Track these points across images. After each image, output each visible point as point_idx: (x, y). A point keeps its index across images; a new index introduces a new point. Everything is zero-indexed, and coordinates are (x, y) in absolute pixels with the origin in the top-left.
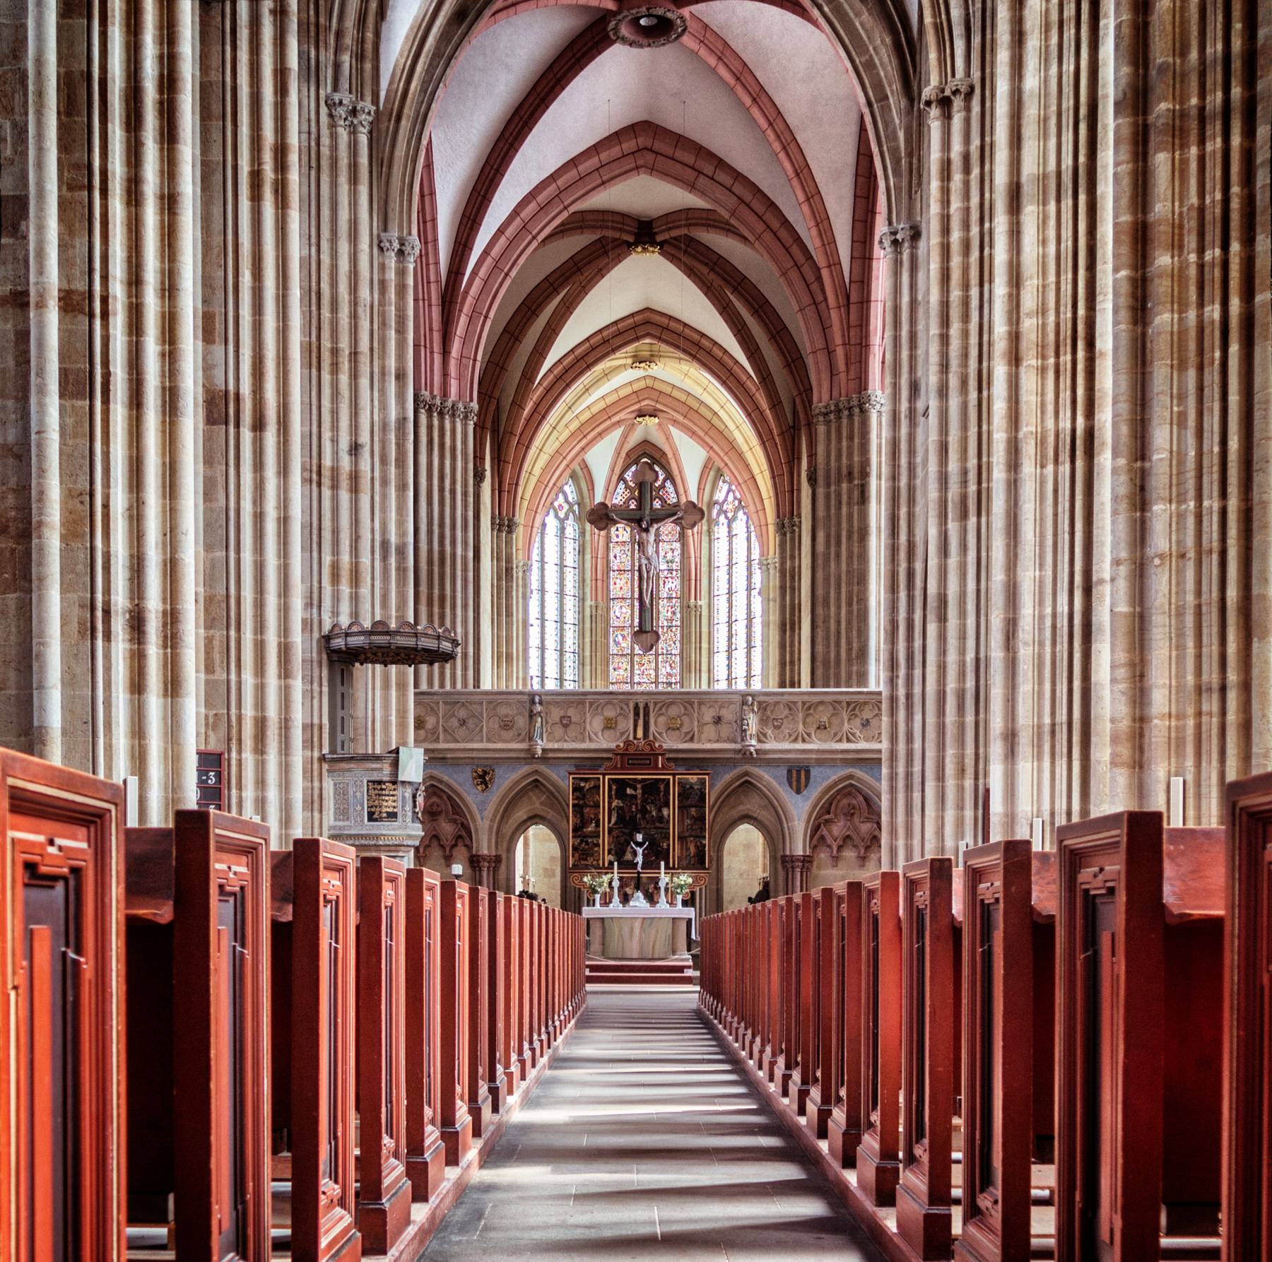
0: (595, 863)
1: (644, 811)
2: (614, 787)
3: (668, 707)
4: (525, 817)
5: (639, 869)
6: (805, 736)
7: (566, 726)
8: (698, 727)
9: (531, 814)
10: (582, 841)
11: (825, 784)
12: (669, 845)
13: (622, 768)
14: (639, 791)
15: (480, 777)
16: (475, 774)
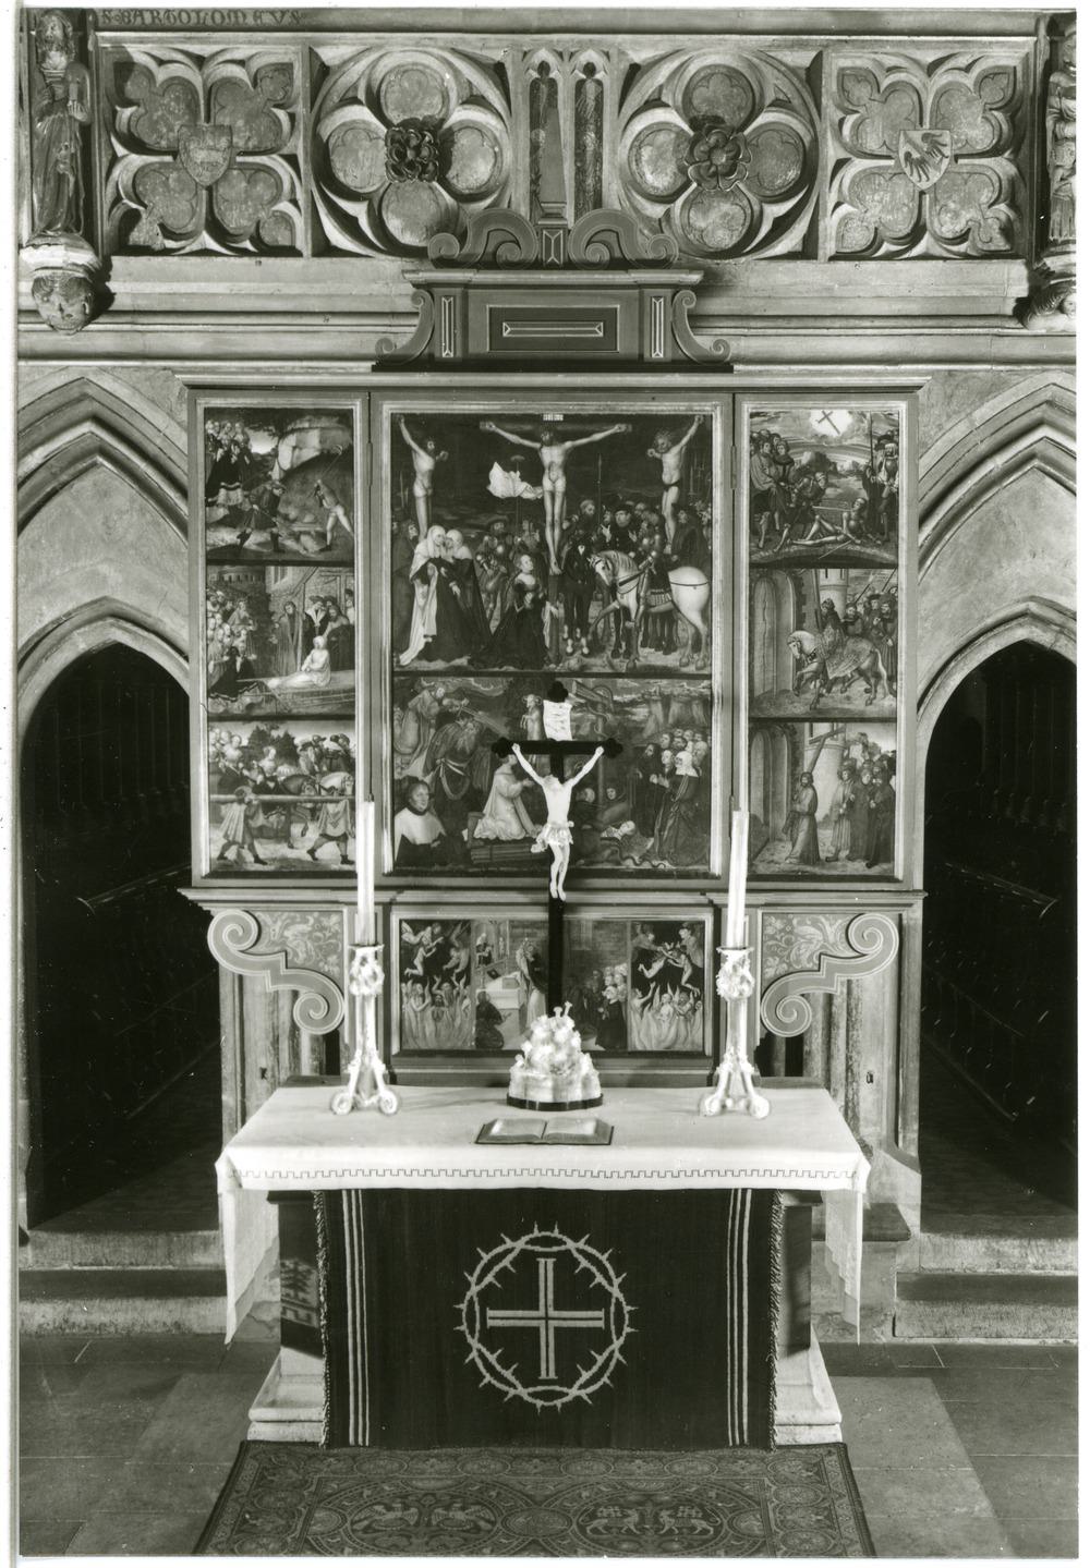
1: (578, 586)
2: (424, 463)
10: (260, 739)
12: (704, 764)
14: (555, 481)
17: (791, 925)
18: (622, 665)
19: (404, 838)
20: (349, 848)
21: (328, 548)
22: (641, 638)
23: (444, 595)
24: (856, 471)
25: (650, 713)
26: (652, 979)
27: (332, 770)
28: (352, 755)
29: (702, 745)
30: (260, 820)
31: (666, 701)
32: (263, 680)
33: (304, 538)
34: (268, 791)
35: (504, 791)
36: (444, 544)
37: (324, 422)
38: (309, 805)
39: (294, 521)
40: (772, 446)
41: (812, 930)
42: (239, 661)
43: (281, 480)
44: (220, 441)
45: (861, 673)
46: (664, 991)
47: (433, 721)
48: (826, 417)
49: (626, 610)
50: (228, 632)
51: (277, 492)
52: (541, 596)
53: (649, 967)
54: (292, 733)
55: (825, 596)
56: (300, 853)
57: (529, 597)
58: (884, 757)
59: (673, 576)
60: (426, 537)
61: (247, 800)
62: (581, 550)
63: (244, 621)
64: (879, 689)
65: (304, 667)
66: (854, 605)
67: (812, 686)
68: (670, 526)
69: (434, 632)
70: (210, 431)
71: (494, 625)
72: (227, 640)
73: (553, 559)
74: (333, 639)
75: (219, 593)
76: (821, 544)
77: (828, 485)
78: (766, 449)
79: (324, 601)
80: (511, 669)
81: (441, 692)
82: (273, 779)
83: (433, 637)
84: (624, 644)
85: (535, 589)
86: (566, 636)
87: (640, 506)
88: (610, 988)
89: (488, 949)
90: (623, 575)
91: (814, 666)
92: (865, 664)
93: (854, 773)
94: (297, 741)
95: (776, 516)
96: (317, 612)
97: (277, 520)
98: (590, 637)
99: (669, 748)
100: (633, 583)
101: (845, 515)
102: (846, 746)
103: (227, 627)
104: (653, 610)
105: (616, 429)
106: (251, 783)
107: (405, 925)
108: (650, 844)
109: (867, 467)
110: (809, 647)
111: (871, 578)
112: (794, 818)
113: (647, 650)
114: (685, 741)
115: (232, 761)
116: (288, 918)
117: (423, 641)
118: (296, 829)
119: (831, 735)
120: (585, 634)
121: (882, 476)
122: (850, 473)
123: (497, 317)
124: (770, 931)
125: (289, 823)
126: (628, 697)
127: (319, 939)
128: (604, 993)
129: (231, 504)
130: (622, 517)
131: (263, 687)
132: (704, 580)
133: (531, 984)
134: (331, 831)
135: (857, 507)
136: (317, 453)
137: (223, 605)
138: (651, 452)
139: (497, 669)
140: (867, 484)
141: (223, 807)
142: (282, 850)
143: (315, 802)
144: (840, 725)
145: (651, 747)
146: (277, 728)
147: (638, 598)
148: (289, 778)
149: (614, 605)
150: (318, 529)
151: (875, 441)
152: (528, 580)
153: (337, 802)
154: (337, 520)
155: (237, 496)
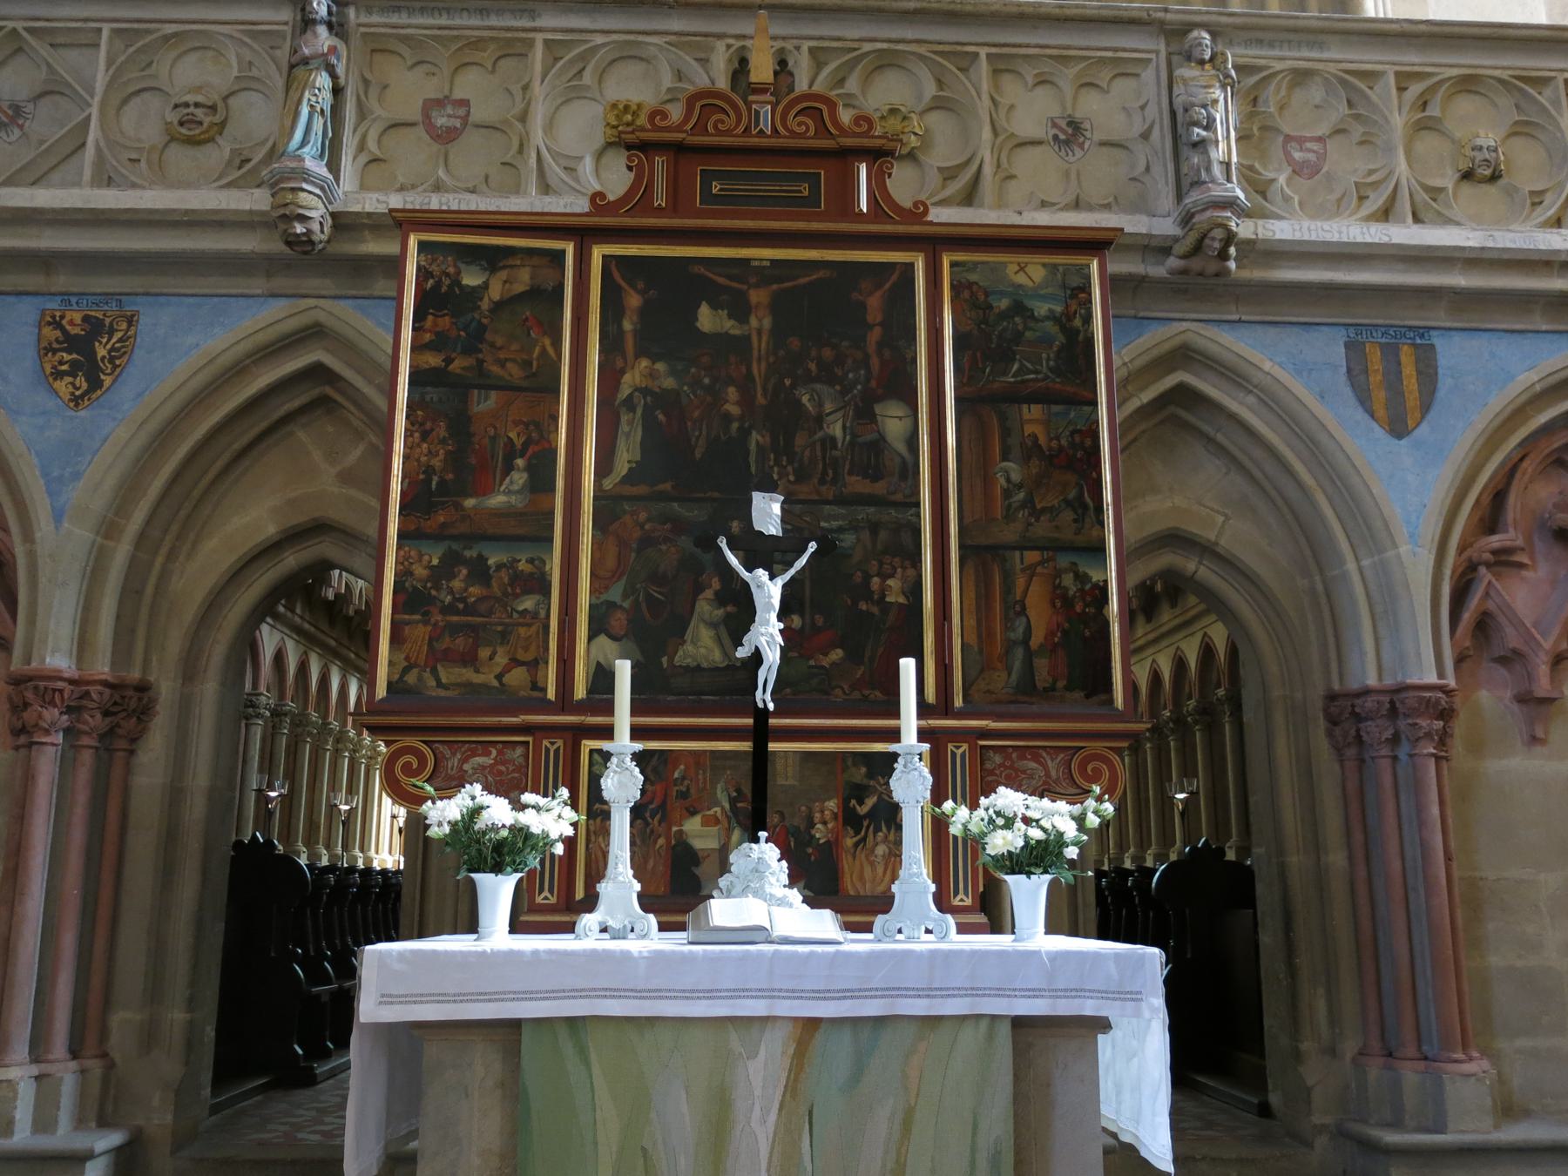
0: (517, 677)
2: (634, 300)
3: (867, 80)
4: (271, 530)
5: (764, 698)
6: (1423, 196)
7: (446, 137)
8: (996, 150)
9: (299, 518)
10: (451, 562)
11: (1498, 401)
12: (916, 590)
13: (674, 207)
14: (761, 322)
15: (71, 343)
16: (51, 334)
17: (1011, 759)
18: (828, 492)
19: (598, 663)
20: (540, 674)
21: (534, 375)
22: (847, 467)
23: (649, 424)
24: (1051, 316)
25: (858, 540)
26: (865, 817)
27: (527, 591)
28: (548, 577)
29: (911, 572)
30: (445, 643)
31: (874, 528)
32: (458, 499)
33: (509, 365)
34: (458, 613)
35: (707, 617)
36: (651, 375)
37: (536, 261)
38: (499, 628)
39: (500, 348)
40: (972, 292)
41: (1033, 765)
42: (435, 479)
43: (491, 311)
44: (431, 273)
45: (1068, 503)
46: (878, 829)
47: (634, 546)
48: (1022, 269)
49: (833, 439)
50: (425, 451)
51: (485, 321)
52: (747, 425)
53: (861, 803)
54: (485, 553)
55: (1028, 429)
56: (487, 677)
57: (735, 425)
58: (1096, 586)
59: (878, 409)
60: (633, 368)
61: (433, 620)
62: (787, 382)
63: (443, 441)
64: (1087, 520)
65: (502, 488)
66: (1058, 438)
67: (1020, 515)
68: (875, 363)
69: (638, 458)
70: (423, 263)
71: (698, 455)
72: (424, 459)
73: (759, 389)
74: (535, 462)
75: (419, 413)
76: (1023, 382)
77: (1026, 328)
78: (966, 294)
79: (527, 425)
80: (716, 495)
81: (643, 516)
82: (463, 600)
83: (636, 462)
84: (830, 472)
85: (741, 418)
86: (772, 463)
87: (845, 344)
88: (819, 826)
89: (686, 782)
90: (828, 407)
91: (1021, 495)
92: (1072, 494)
93: (1067, 602)
94: (490, 562)
95: (978, 355)
96: (518, 435)
97: (484, 347)
98: (796, 465)
99: (877, 575)
100: (840, 414)
101: (1044, 355)
102: (1058, 574)
103: (425, 446)
104: (860, 440)
105: (821, 274)
106: (439, 604)
107: (596, 756)
108: (859, 673)
109: (1062, 314)
110: (1016, 477)
111: (1072, 414)
112: (1010, 646)
113: (854, 478)
114: (895, 569)
115: (420, 580)
116: (469, 750)
117: (627, 466)
118: (484, 653)
119: (1041, 563)
120: (790, 462)
121: (1077, 322)
122: (1047, 318)
123: (707, 177)
124: (988, 766)
125: (476, 646)
126: (835, 524)
127: (500, 773)
128: (813, 832)
129: (438, 329)
130: (827, 353)
131: (458, 506)
132: (909, 412)
133: (733, 820)
134: (521, 655)
135: (1055, 349)
136: (528, 288)
137: (421, 425)
138: (855, 296)
139: (702, 495)
140: (1064, 329)
141: (407, 628)
142: (468, 674)
143: (506, 625)
144: (1051, 553)
145: (859, 573)
146: (471, 548)
147: (844, 427)
148: (480, 599)
149: (820, 434)
150: (525, 357)
151: (1069, 292)
152: (734, 410)
153: (529, 625)
154: (544, 350)
155: (445, 322)
